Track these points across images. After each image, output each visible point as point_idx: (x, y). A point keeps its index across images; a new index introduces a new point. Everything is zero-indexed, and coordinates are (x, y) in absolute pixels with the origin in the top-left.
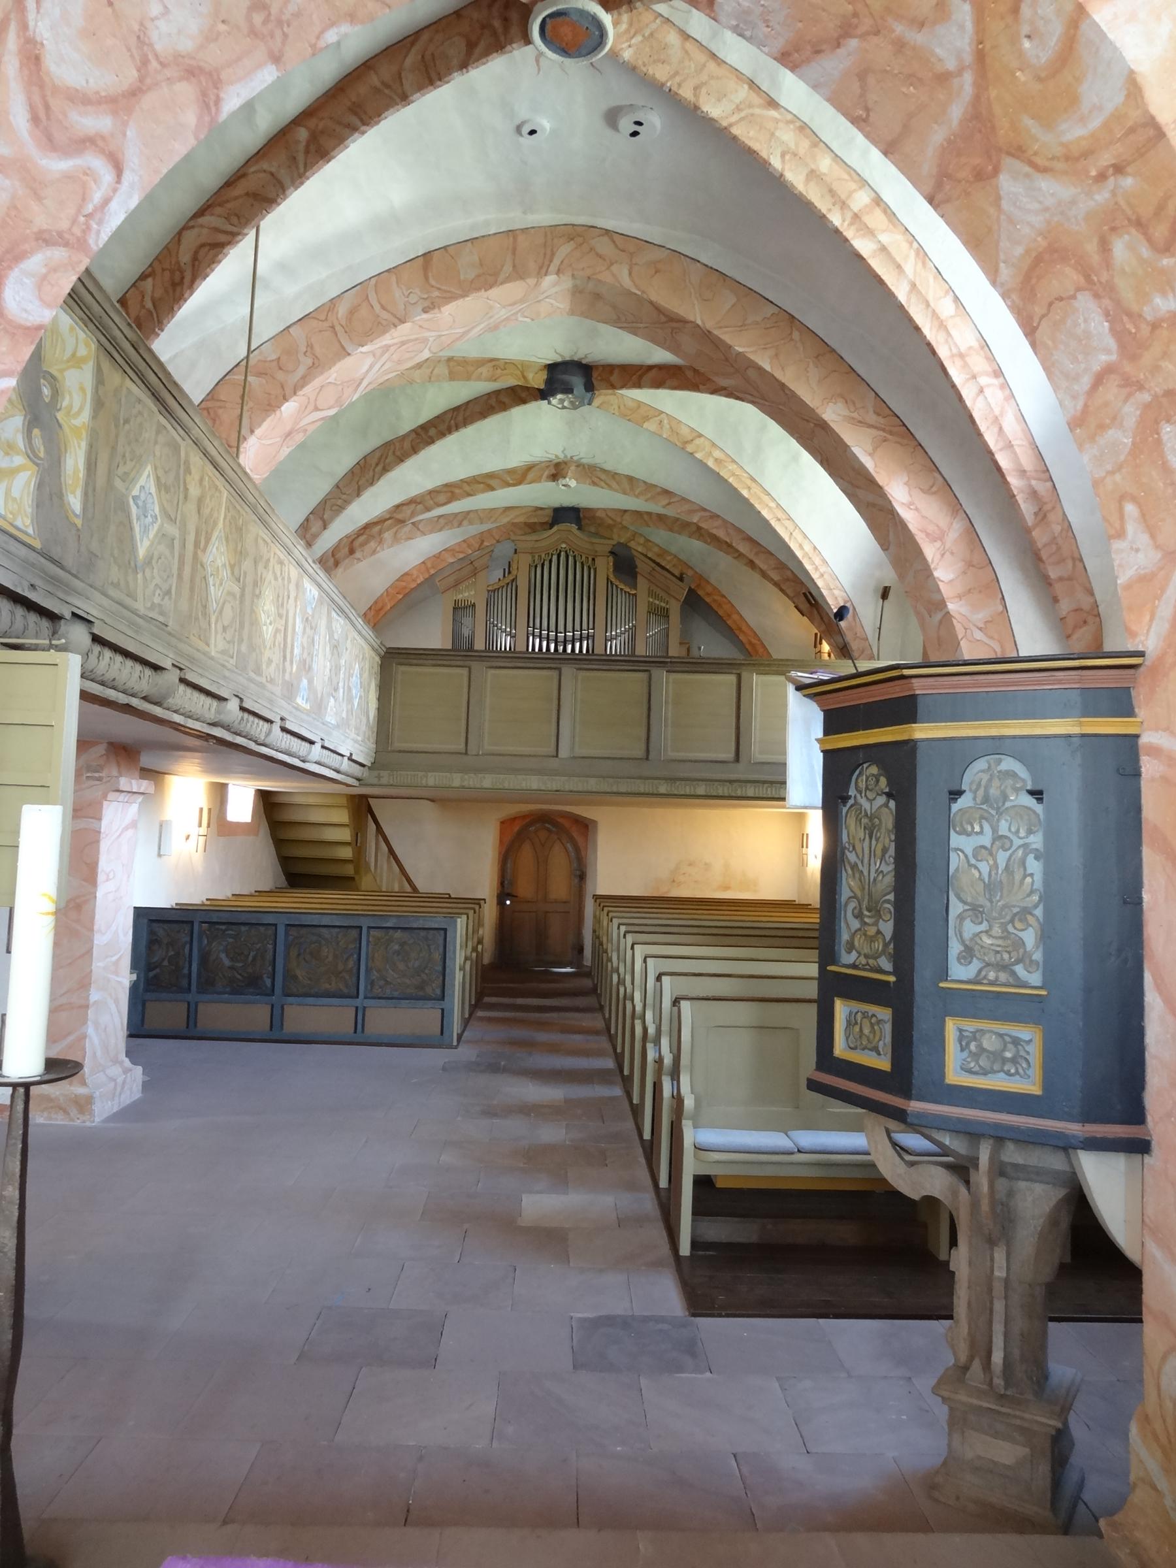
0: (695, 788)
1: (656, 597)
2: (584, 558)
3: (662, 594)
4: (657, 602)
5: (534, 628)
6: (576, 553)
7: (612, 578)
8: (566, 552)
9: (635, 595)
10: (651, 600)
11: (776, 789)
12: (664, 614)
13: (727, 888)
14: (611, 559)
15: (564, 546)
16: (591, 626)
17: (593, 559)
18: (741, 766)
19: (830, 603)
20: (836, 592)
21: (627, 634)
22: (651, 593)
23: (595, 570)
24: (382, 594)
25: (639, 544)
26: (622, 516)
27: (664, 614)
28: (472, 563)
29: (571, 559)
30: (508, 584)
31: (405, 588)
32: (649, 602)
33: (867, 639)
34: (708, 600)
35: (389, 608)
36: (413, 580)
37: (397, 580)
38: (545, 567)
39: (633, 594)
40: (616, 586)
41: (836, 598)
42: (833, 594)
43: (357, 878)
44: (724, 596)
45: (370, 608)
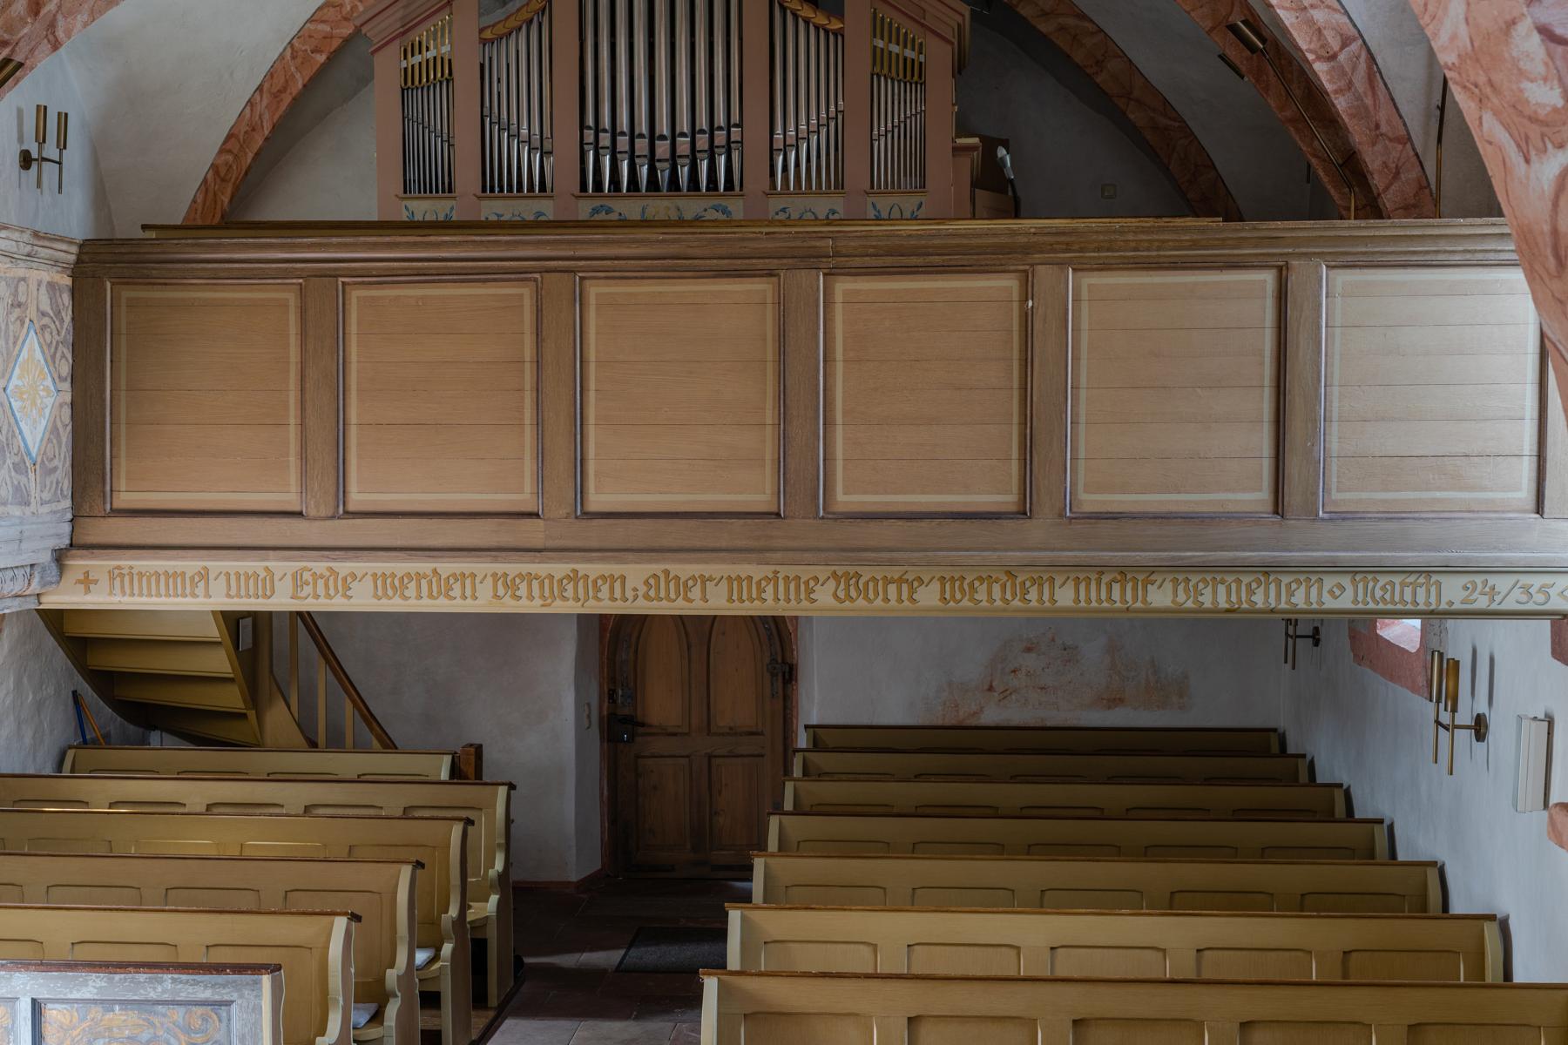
0: (912, 591)
3: (907, 26)
4: (895, 48)
5: (597, 131)
10: (880, 44)
11: (1135, 589)
12: (913, 75)
13: (1115, 701)
16: (735, 118)
18: (1035, 530)
19: (1304, 46)
20: (1319, 16)
21: (823, 131)
22: (878, 27)
24: (281, 56)
27: (913, 75)
30: (531, 21)
31: (328, 37)
32: (875, 47)
33: (1410, 139)
34: (1044, 27)
35: (300, 86)
36: (346, 19)
37: (310, 20)
41: (1319, 30)
42: (1311, 22)
43: (252, 714)
44: (1082, 16)
45: (260, 88)
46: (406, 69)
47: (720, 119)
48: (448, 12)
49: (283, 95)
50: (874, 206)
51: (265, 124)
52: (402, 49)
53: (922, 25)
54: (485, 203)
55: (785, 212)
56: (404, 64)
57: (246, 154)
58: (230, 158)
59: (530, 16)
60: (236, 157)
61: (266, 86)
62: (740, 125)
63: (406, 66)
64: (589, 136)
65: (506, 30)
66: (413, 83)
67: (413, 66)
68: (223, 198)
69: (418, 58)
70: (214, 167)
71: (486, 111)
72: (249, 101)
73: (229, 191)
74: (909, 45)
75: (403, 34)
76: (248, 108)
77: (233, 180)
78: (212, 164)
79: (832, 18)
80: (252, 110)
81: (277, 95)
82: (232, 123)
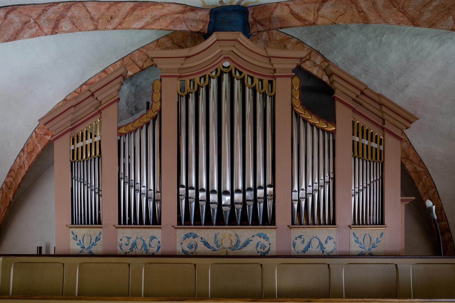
1: (365, 133)
2: (256, 81)
6: (245, 73)
7: (300, 110)
8: (230, 73)
9: (333, 133)
10: (357, 139)
14: (296, 80)
15: (226, 64)
17: (271, 82)
23: (273, 98)
24: (31, 137)
25: (315, 65)
26: (319, 10)
28: (93, 95)
29: (237, 84)
35: (40, 149)
38: (201, 97)
39: (329, 132)
40: (305, 121)
45: (23, 150)
46: (73, 150)
47: (261, 181)
48: (99, 117)
49: (33, 154)
50: (354, 234)
51: (26, 165)
52: (72, 138)
53: (383, 129)
54: (120, 230)
55: (301, 238)
56: (72, 147)
57: (18, 178)
58: (12, 179)
59: (148, 120)
60: (14, 179)
61: (26, 149)
62: (273, 185)
63: (73, 148)
64: (183, 190)
65: (134, 128)
66: (77, 159)
67: (78, 148)
68: (10, 195)
69: (80, 144)
70: (5, 182)
71: (122, 176)
72: (18, 155)
73: (12, 193)
74: (374, 140)
75: (72, 129)
76: (18, 158)
77: (13, 188)
78: (5, 182)
79: (328, 124)
80: (20, 159)
81: (30, 153)
82: (12, 165)
